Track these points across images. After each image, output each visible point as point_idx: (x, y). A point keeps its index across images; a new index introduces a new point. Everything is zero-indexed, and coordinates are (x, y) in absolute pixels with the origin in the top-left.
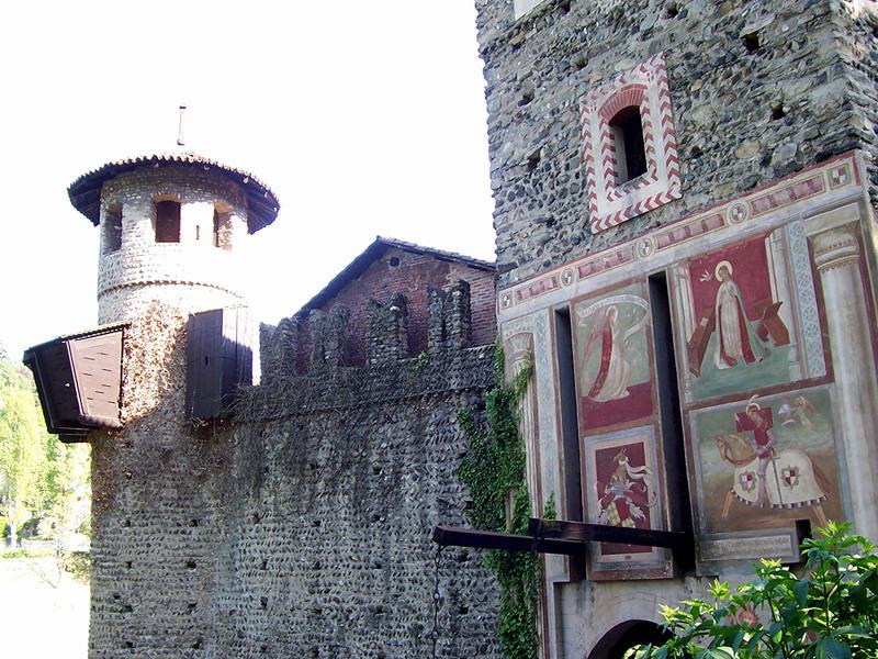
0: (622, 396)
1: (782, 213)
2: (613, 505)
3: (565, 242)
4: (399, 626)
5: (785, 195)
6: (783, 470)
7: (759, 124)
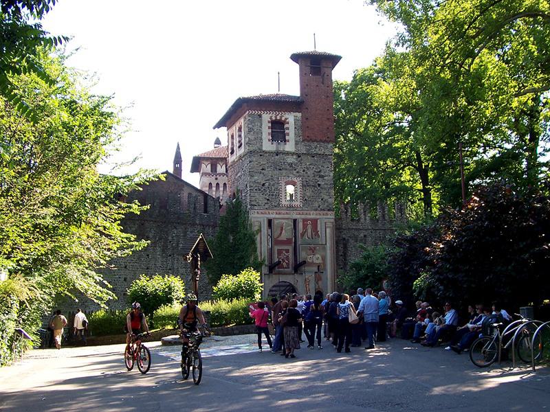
1: (321, 217)
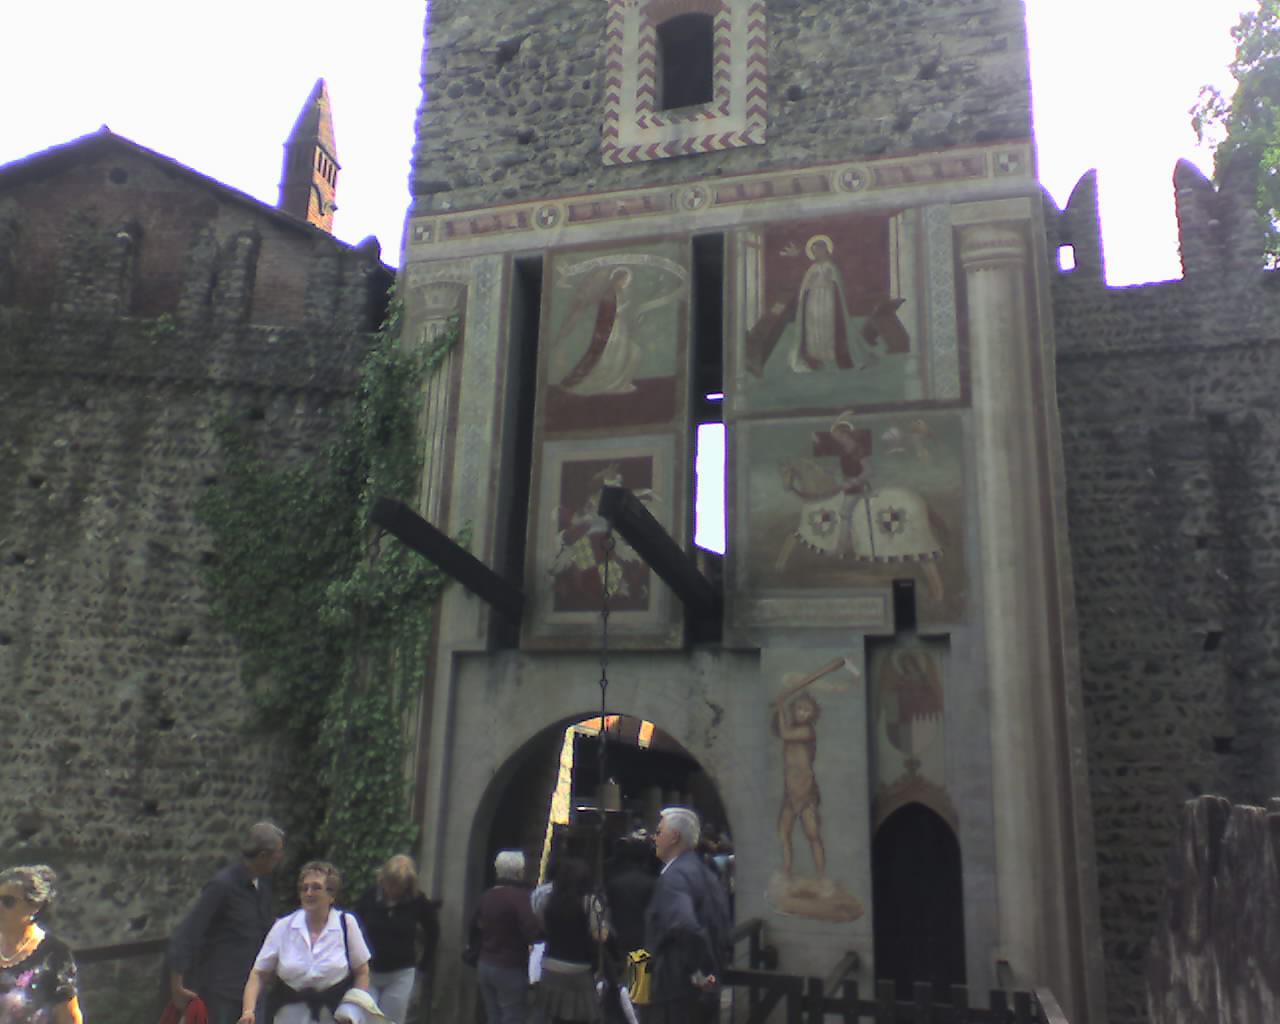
0: (623, 390)
1: (921, 192)
2: (585, 541)
3: (550, 170)
4: (28, 745)
5: (928, 171)
6: (880, 514)
7: (900, 78)
